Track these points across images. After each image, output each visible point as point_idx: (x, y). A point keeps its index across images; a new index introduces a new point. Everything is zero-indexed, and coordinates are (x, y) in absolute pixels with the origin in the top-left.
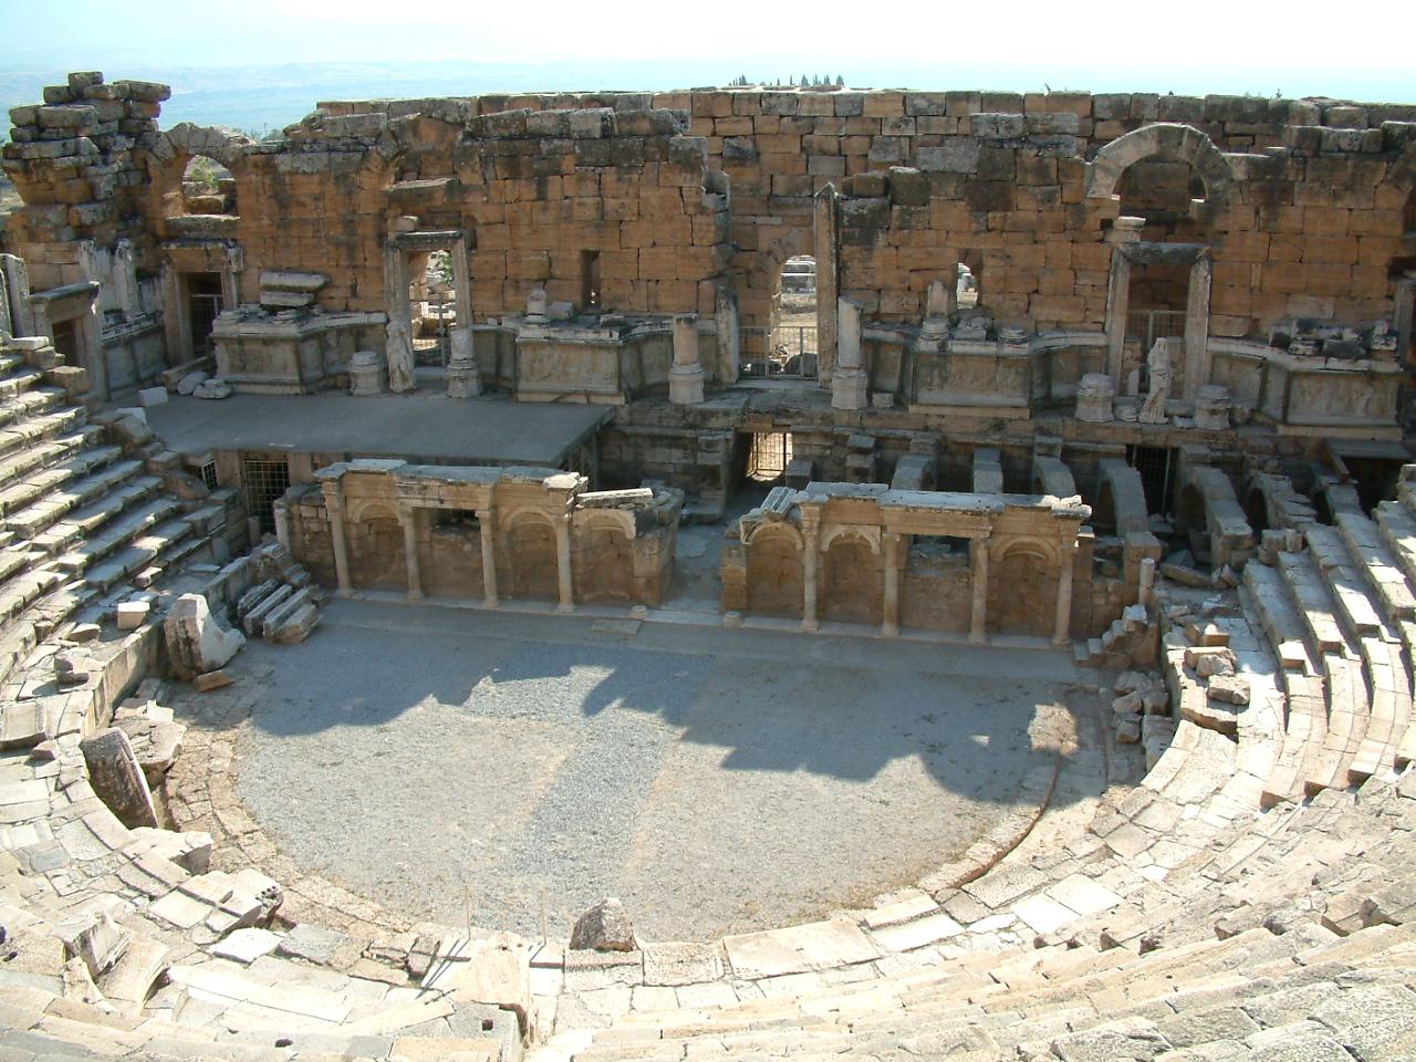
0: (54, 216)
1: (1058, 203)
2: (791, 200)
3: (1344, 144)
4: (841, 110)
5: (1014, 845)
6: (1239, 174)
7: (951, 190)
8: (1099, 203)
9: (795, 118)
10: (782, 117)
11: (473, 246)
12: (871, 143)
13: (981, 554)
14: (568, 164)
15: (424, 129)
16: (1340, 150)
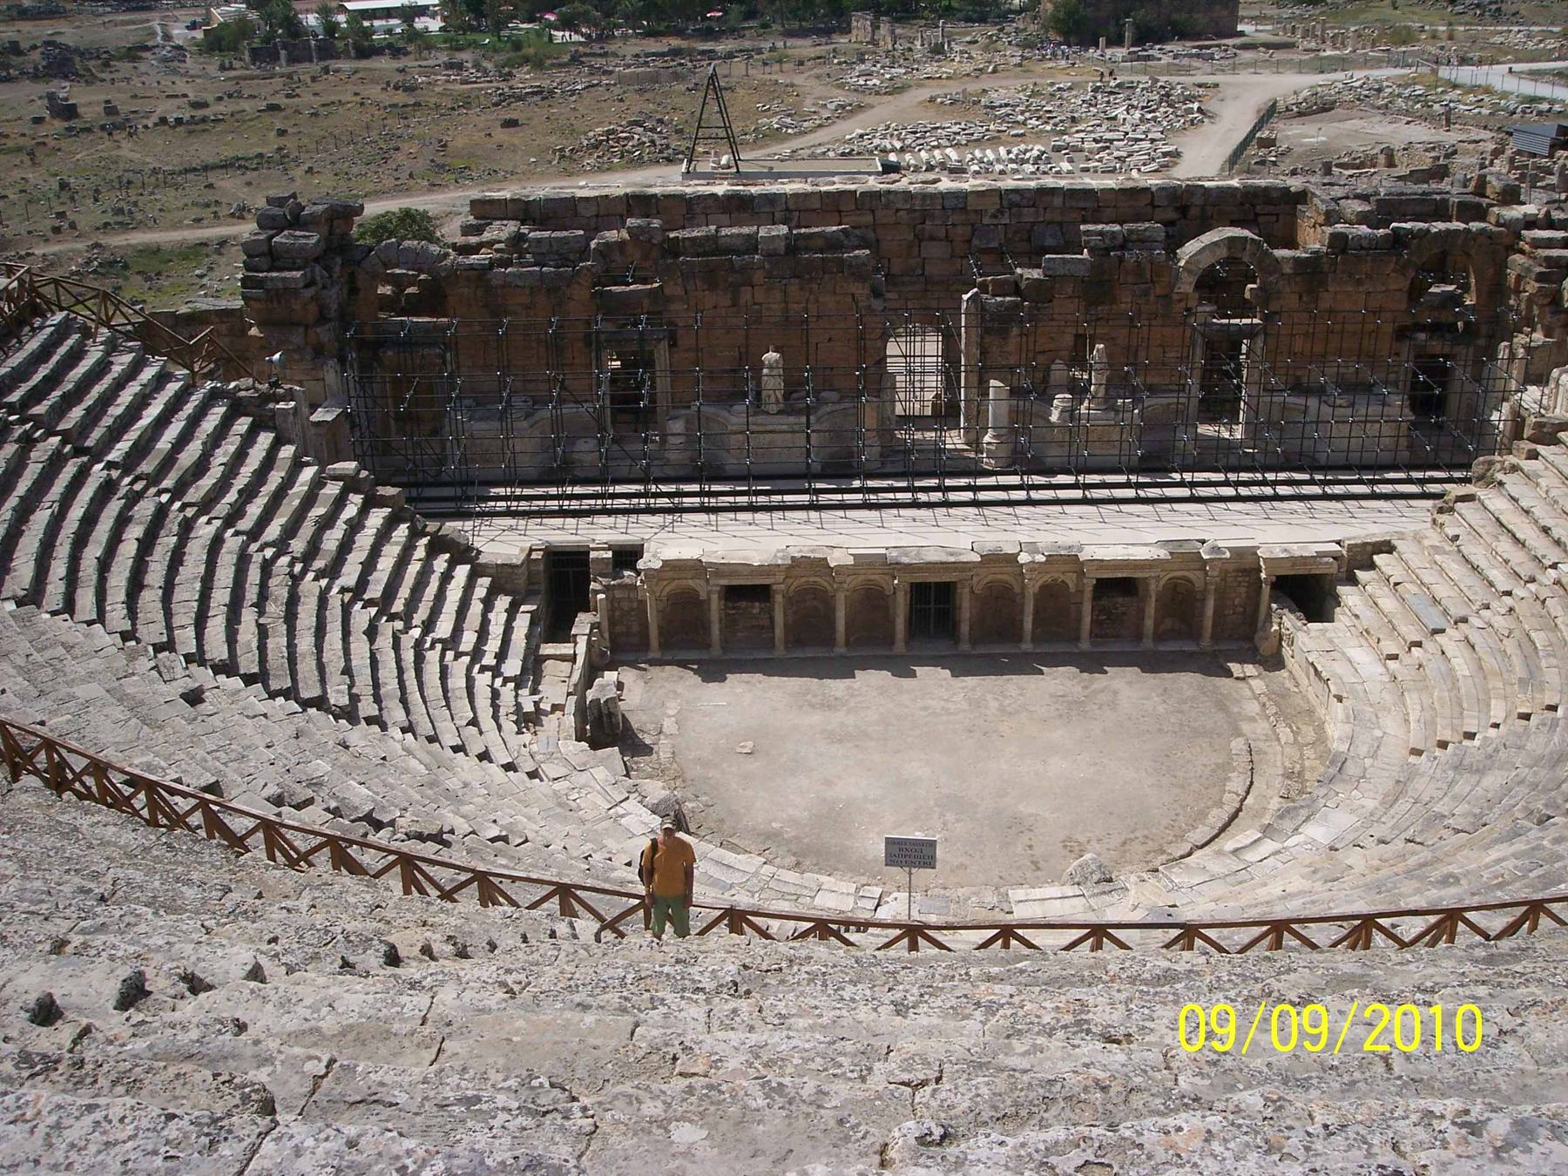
0: (297, 337)
1: (1152, 298)
2: (906, 279)
3: (1365, 243)
4: (948, 204)
5: (1248, 793)
6: (1287, 270)
7: (1070, 291)
8: (1184, 297)
9: (910, 211)
10: (898, 210)
11: (673, 344)
12: (974, 230)
13: (1153, 587)
14: (758, 277)
15: (630, 249)
16: (1362, 248)
